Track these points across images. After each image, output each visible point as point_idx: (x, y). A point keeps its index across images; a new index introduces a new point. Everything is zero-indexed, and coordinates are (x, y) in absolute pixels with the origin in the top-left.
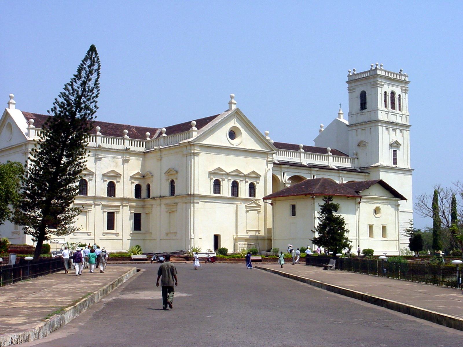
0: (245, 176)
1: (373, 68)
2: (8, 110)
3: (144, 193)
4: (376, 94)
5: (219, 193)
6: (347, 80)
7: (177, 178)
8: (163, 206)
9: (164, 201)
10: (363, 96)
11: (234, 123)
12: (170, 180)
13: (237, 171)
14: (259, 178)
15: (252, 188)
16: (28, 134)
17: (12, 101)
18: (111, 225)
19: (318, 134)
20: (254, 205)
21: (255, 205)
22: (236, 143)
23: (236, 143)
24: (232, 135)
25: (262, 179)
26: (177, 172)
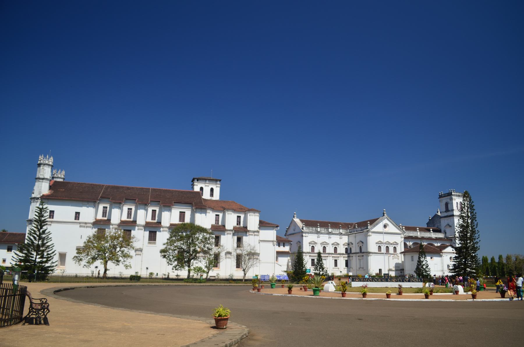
0: (391, 244)
1: (450, 192)
2: (294, 219)
3: (349, 252)
4: (452, 203)
5: (381, 251)
6: (439, 197)
7: (362, 245)
8: (357, 257)
9: (358, 255)
10: (447, 204)
11: (386, 221)
12: (360, 246)
13: (388, 242)
14: (398, 245)
15: (395, 248)
16: (303, 229)
17: (295, 215)
18: (336, 265)
19: (428, 221)
20: (396, 256)
21: (397, 256)
22: (386, 230)
23: (387, 230)
24: (385, 226)
25: (399, 245)
26: (363, 243)
